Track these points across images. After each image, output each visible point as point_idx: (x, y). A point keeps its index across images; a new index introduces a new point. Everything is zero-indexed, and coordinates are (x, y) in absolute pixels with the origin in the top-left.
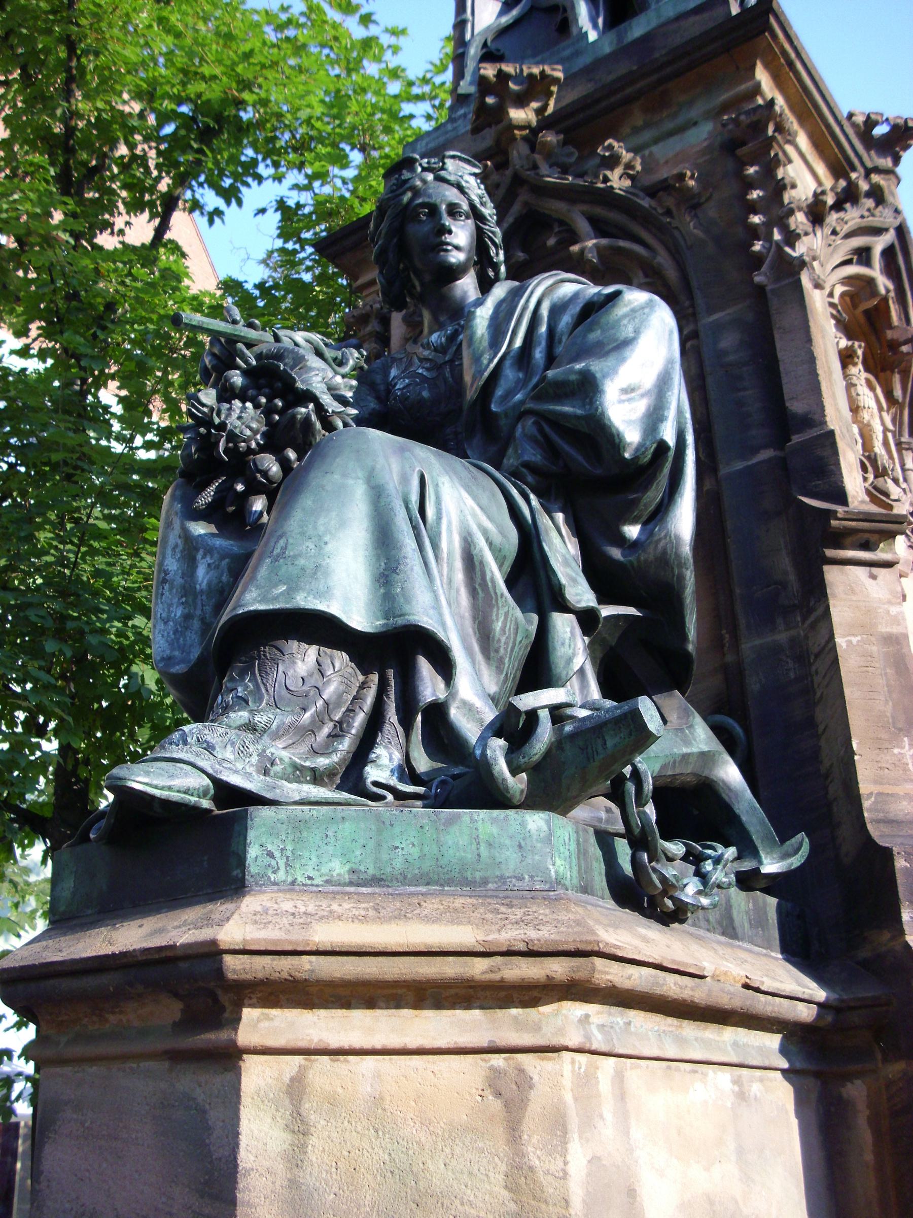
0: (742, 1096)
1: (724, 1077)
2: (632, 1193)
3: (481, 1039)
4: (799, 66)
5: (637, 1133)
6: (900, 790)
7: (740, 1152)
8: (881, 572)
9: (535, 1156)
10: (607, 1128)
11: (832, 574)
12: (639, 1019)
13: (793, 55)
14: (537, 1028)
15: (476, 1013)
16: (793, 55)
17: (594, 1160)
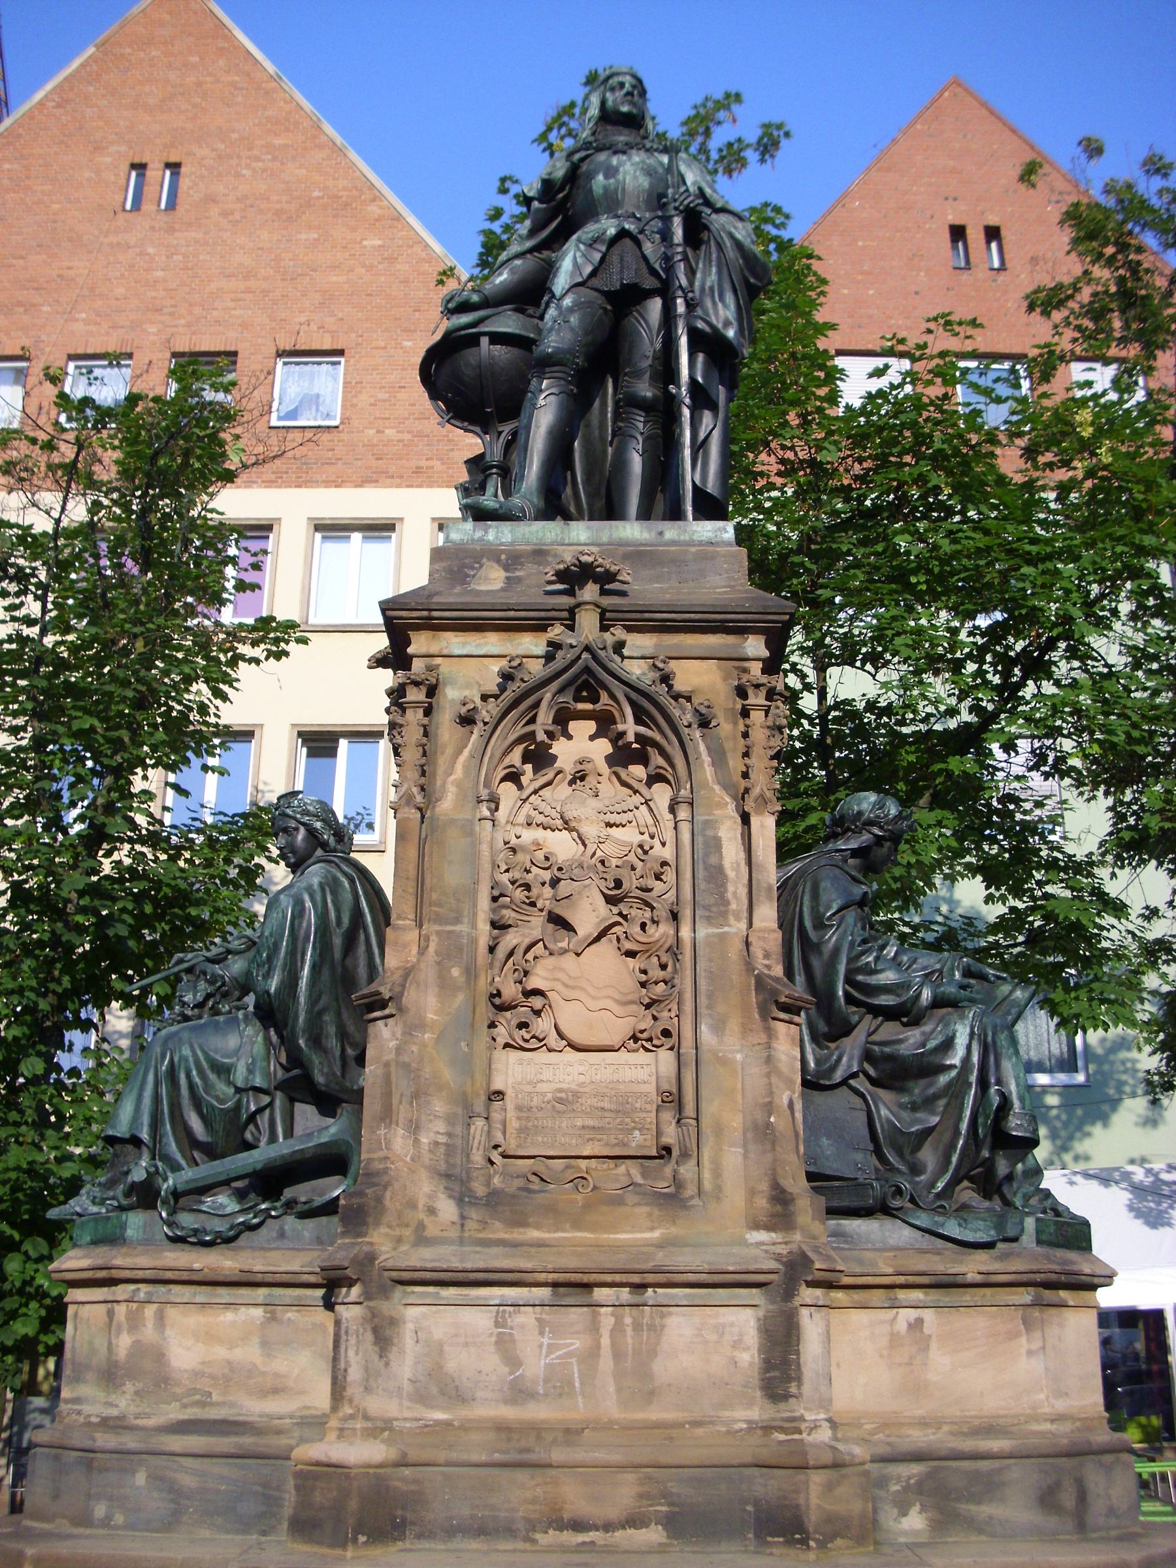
0: (273, 1318)
1: (258, 1312)
2: (163, 1355)
3: (101, 1298)
4: (435, 614)
5: (169, 1332)
6: (375, 1156)
7: (265, 1344)
8: (390, 1021)
9: (114, 1341)
10: (149, 1331)
11: (372, 1029)
12: (176, 1289)
13: (425, 613)
14: (114, 1293)
15: (106, 1289)
16: (425, 613)
17: (137, 1342)
